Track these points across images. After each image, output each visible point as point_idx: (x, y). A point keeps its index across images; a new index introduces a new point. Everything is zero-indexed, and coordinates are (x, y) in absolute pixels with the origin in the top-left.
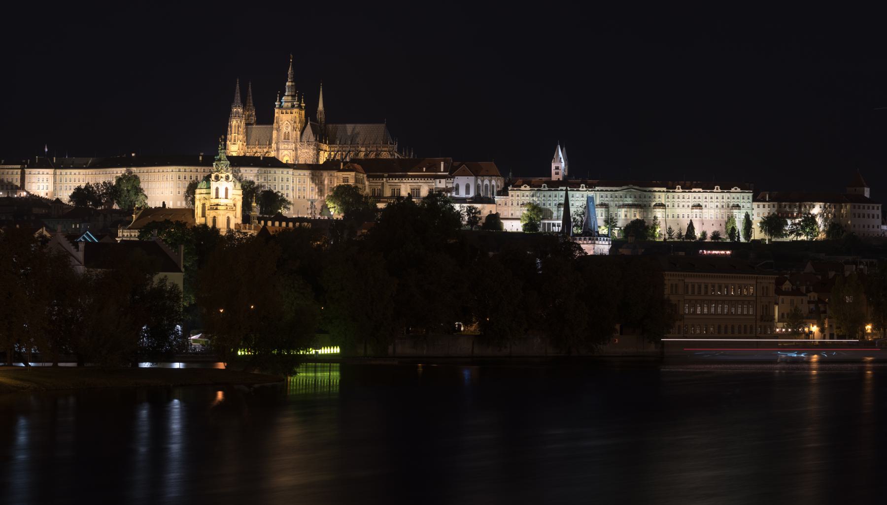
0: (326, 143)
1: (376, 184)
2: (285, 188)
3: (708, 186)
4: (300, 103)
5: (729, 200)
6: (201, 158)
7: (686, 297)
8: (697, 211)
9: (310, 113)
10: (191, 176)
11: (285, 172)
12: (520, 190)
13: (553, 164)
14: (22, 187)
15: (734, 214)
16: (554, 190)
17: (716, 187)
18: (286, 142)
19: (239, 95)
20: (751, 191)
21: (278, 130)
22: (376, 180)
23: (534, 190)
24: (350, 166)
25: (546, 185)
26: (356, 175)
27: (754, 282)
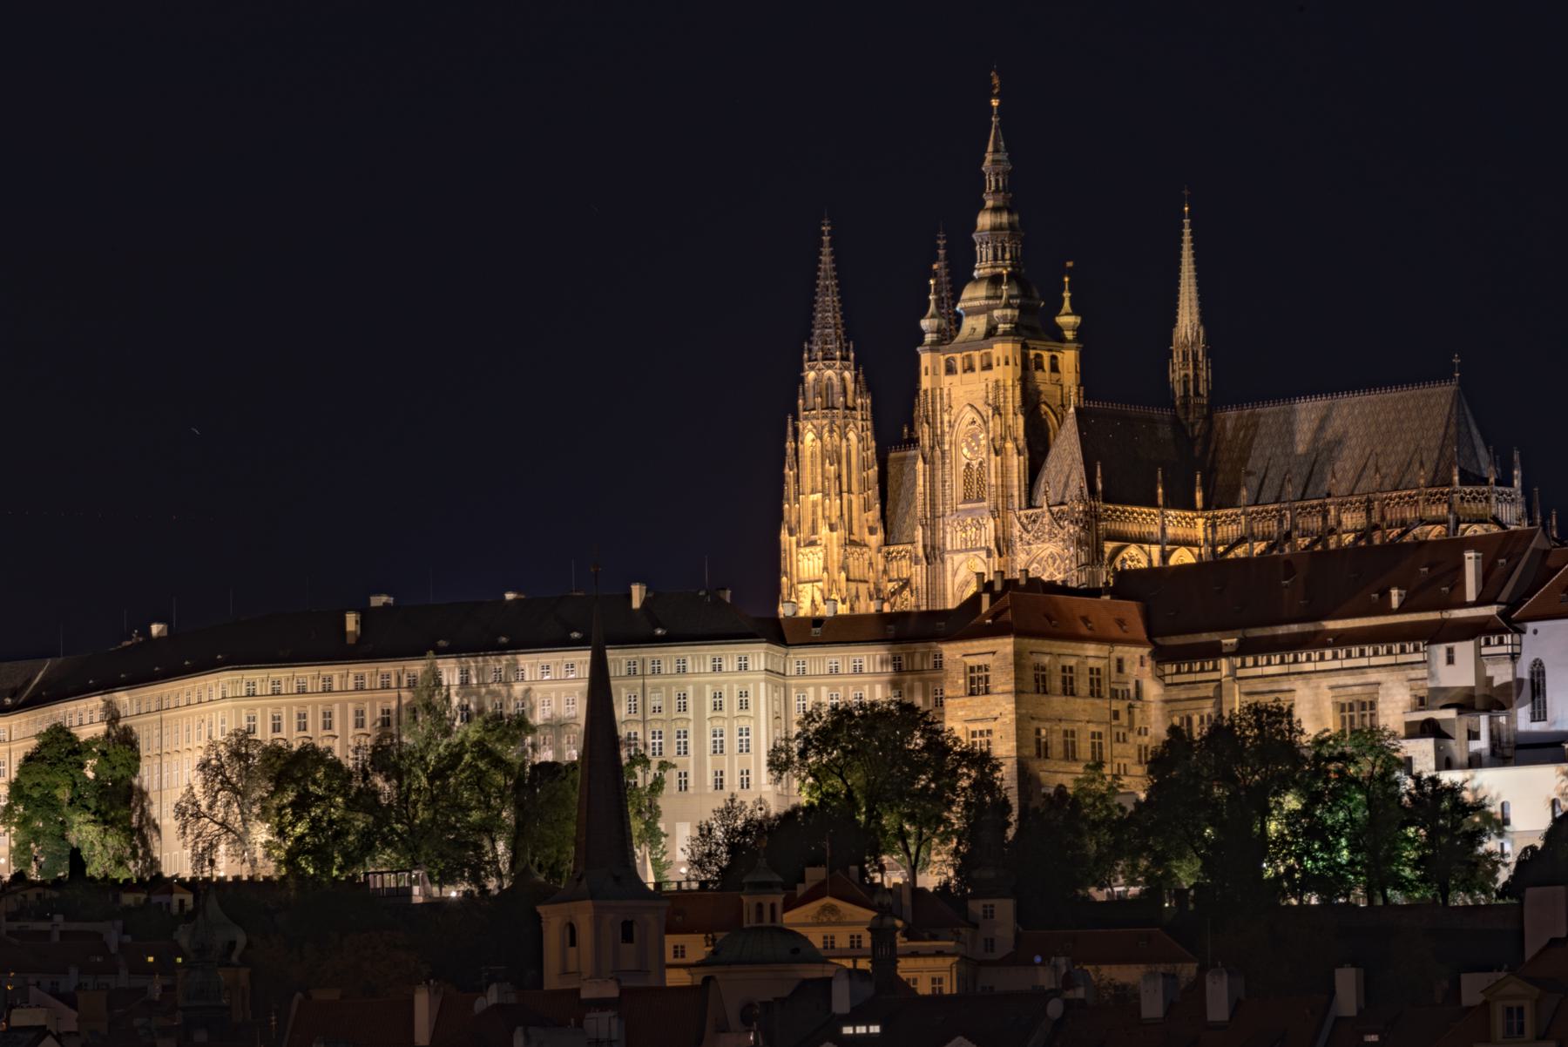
0: (1192, 507)
1: (1194, 694)
2: (732, 742)
4: (1057, 309)
6: (351, 622)
10: (302, 716)
11: (730, 664)
18: (969, 512)
22: (1190, 671)
24: (1004, 610)
26: (1018, 654)
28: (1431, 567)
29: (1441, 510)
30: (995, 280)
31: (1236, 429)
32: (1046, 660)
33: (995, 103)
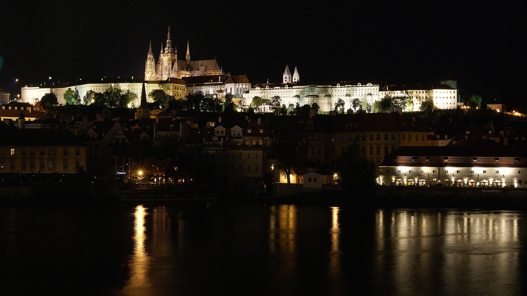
0: (188, 71)
3: (354, 83)
4: (175, 51)
5: (366, 91)
8: (348, 98)
9: (181, 57)
12: (255, 90)
13: (284, 75)
15: (367, 99)
16: (272, 89)
17: (358, 84)
20: (378, 85)
23: (262, 89)
25: (268, 87)
28: (215, 78)
29: (214, 72)
30: (169, 47)
31: (193, 63)
32: (176, 86)
33: (169, 29)
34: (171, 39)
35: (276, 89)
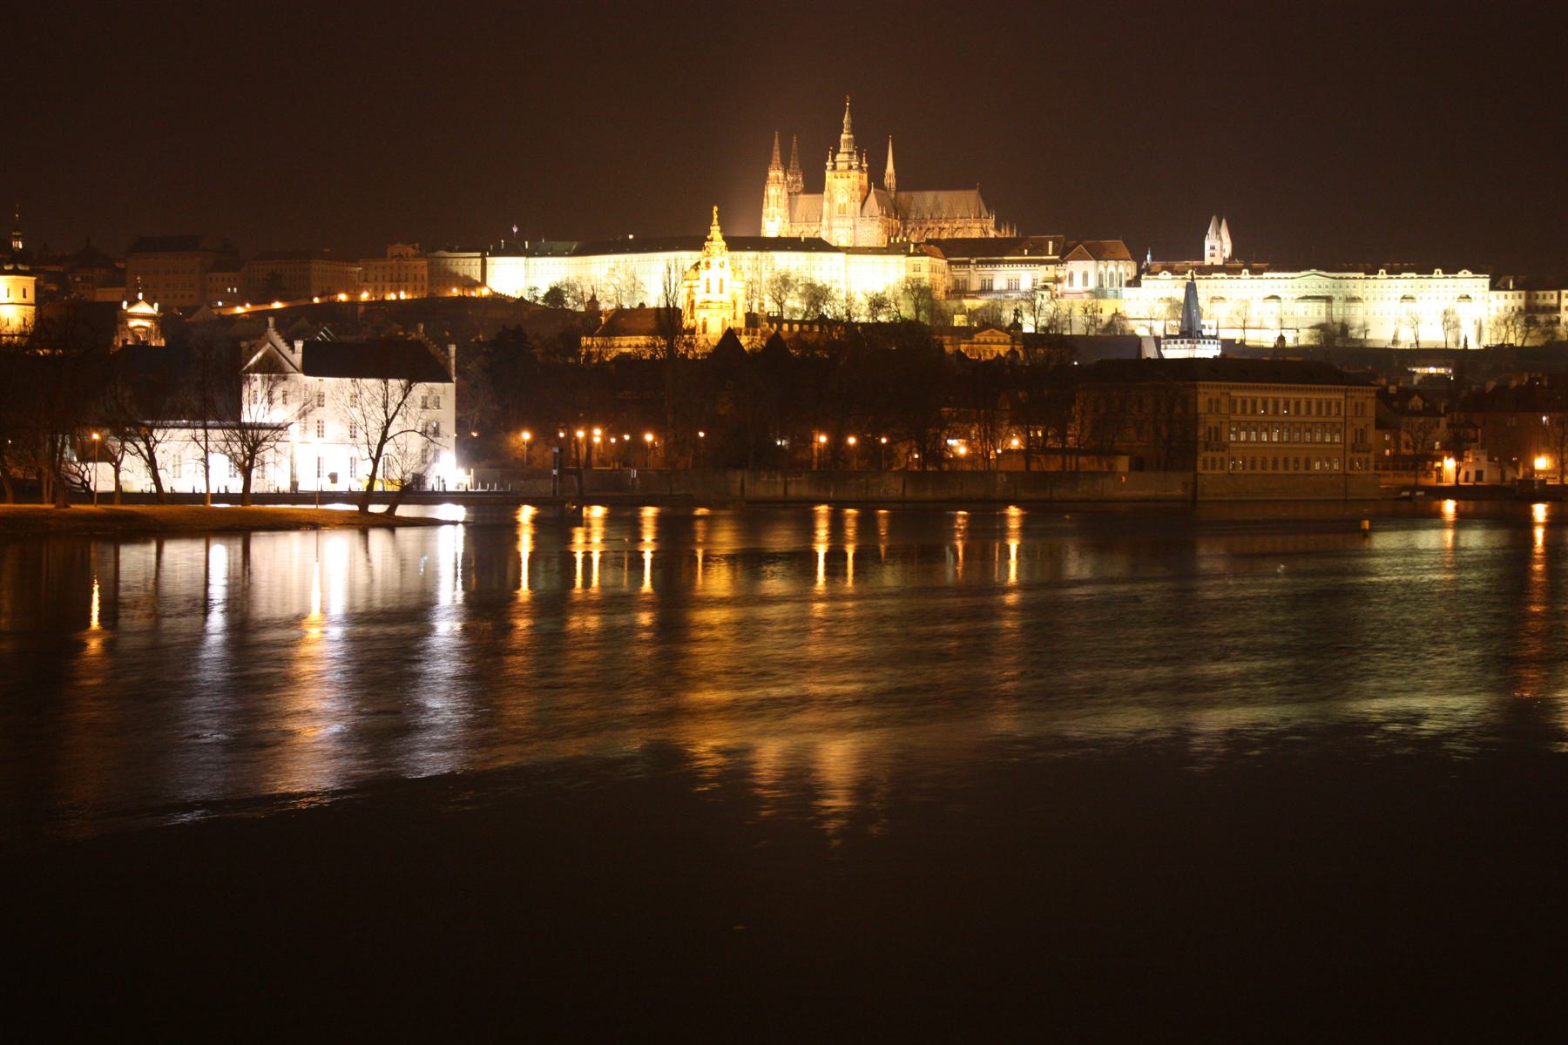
0: (896, 219)
3: (1425, 269)
4: (861, 162)
5: (1455, 289)
7: (1233, 418)
9: (875, 176)
12: (1157, 279)
14: (483, 283)
17: (1436, 271)
19: (778, 153)
20: (1488, 276)
21: (831, 200)
27: (1342, 397)
29: (978, 225)
34: (853, 131)
35: (1216, 278)
